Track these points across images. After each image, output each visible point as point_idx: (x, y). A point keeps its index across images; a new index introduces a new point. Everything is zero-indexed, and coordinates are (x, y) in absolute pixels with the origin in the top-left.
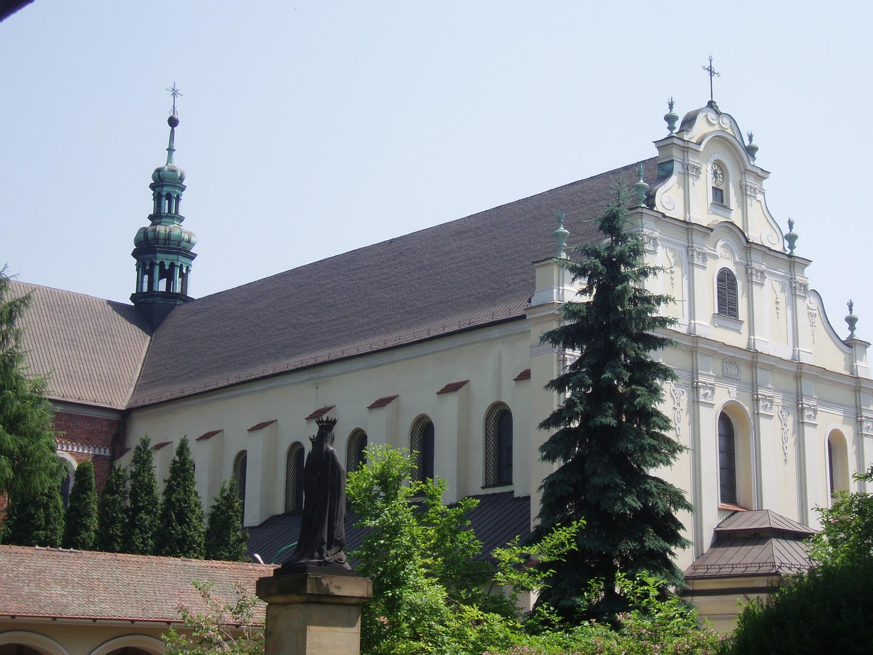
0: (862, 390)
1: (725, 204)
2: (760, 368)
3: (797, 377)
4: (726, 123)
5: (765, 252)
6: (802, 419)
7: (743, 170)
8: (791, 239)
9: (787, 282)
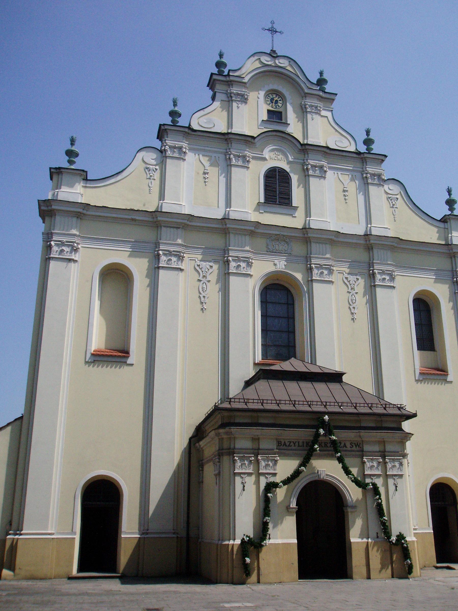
1: (283, 121)
2: (314, 242)
3: (369, 249)
4: (283, 63)
5: (325, 152)
6: (374, 282)
7: (303, 95)
8: (368, 142)
9: (359, 175)
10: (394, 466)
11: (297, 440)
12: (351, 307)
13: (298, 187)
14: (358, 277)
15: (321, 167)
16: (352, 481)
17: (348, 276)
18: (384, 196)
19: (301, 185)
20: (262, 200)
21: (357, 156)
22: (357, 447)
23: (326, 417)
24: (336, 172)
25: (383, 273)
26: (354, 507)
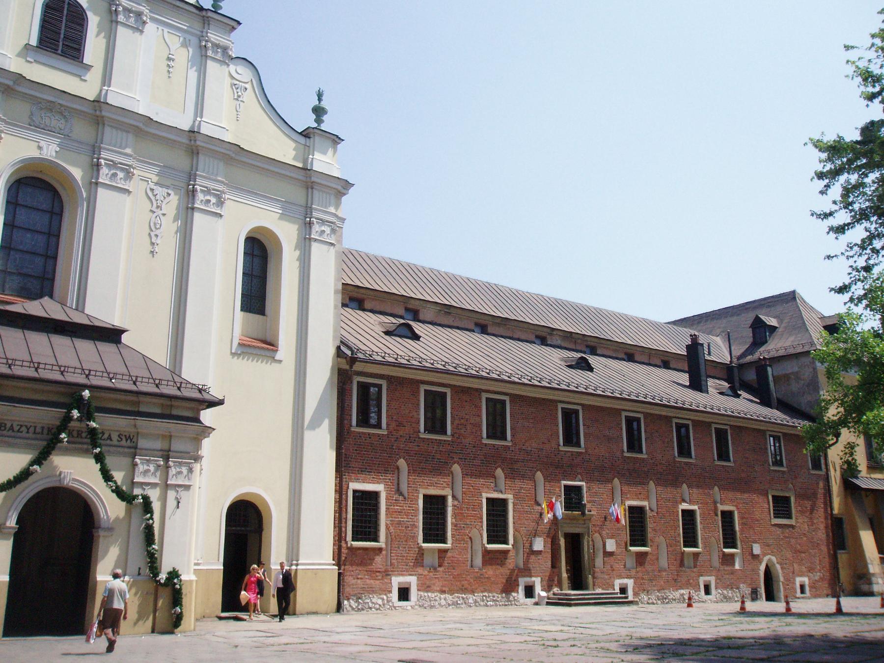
0: (315, 187)
2: (108, 125)
3: (193, 153)
6: (193, 203)
9: (194, 40)
10: (180, 473)
11: (35, 423)
12: (153, 234)
13: (98, 35)
14: (170, 192)
15: (139, 14)
16: (113, 491)
17: (154, 187)
18: (228, 81)
19: (103, 34)
20: (34, 42)
21: (197, 12)
22: (129, 441)
23: (86, 393)
24: (160, 28)
25: (208, 191)
26: (110, 529)
